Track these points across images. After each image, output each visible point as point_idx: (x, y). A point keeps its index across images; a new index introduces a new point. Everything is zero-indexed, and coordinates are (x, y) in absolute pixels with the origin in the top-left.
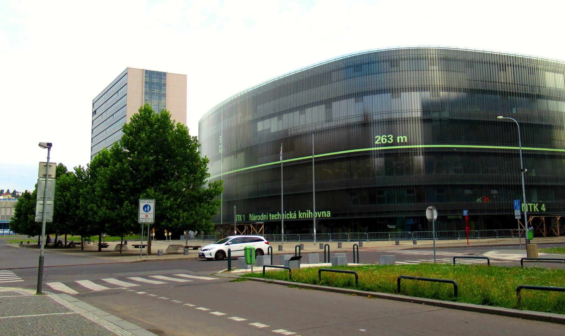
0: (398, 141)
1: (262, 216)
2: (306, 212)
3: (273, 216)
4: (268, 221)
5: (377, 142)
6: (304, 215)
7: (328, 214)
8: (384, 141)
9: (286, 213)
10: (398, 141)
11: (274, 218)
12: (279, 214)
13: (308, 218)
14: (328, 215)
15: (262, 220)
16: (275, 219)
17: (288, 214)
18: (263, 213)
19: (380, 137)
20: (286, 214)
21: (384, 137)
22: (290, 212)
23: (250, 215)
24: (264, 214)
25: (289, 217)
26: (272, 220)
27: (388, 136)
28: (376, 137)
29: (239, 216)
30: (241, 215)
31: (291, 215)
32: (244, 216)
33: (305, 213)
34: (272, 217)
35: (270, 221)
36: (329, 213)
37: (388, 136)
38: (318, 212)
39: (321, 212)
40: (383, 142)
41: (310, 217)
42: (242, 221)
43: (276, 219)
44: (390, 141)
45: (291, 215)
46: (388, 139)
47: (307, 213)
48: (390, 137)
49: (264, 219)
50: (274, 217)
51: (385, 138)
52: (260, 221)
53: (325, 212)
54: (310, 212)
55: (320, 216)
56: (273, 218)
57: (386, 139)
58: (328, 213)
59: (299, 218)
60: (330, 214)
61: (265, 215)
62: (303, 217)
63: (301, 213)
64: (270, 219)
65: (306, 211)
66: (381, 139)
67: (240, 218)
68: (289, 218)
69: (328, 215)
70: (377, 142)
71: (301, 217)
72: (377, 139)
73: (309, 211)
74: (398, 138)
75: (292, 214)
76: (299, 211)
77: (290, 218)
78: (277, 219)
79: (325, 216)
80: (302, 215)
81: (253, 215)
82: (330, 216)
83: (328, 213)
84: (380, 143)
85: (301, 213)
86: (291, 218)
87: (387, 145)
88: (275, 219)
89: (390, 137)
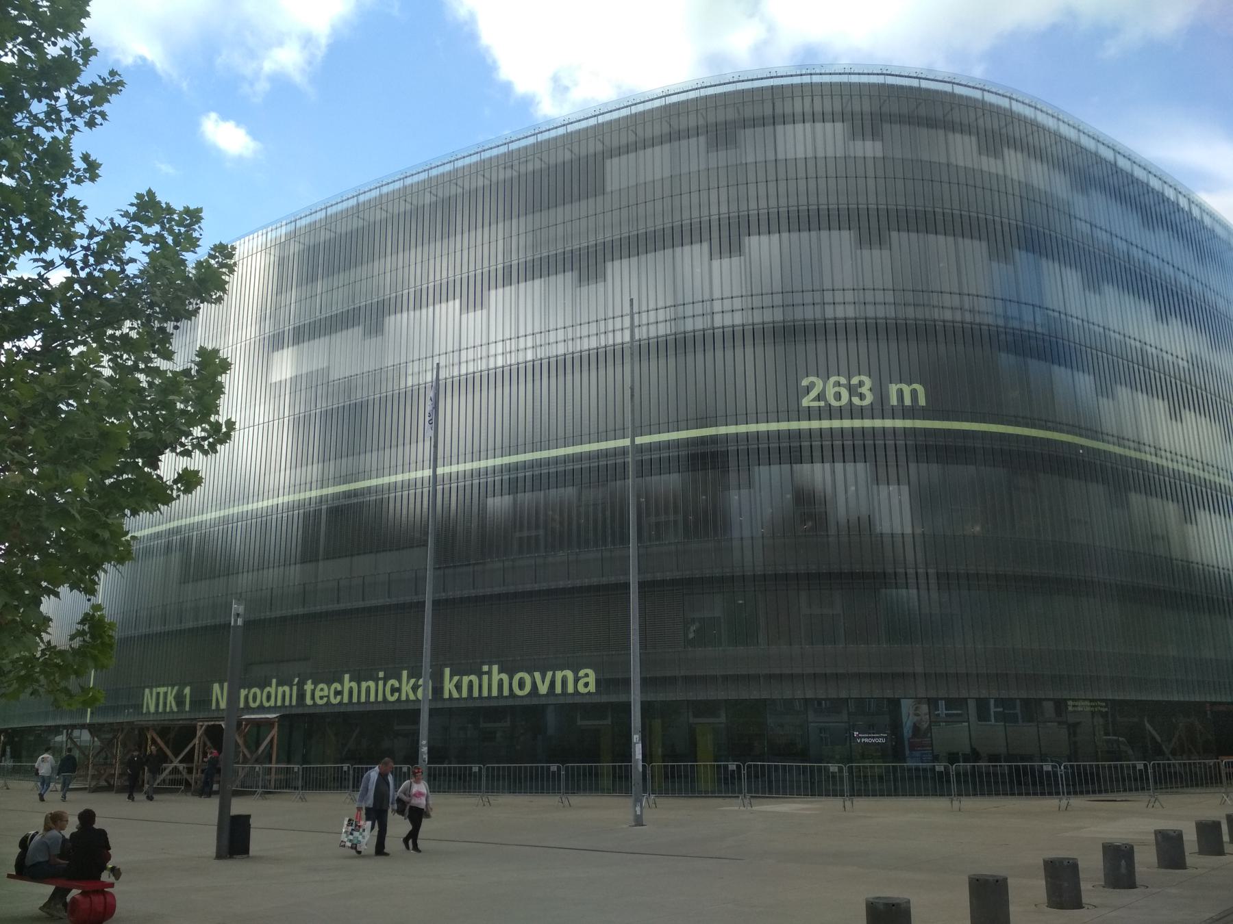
0: (894, 401)
1: (272, 690)
2: (480, 674)
3: (322, 690)
4: (300, 711)
5: (806, 402)
6: (471, 684)
7: (586, 680)
8: (838, 396)
9: (385, 680)
10: (894, 401)
11: (328, 697)
12: (351, 681)
13: (490, 697)
14: (586, 685)
15: (266, 705)
16: (328, 703)
18: (274, 681)
19: (819, 384)
20: (381, 683)
21: (838, 384)
22: (405, 673)
23: (216, 687)
24: (279, 684)
25: (396, 695)
26: (315, 704)
27: (855, 381)
28: (805, 383)
29: (166, 694)
30: (176, 688)
31: (406, 688)
32: (187, 691)
33: (474, 678)
34: (318, 694)
35: (306, 711)
36: (589, 678)
37: (855, 381)
38: (537, 675)
39: (549, 674)
40: (834, 403)
41: (495, 693)
42: (175, 709)
43: (334, 701)
44: (862, 397)
45: (406, 688)
46: (851, 390)
47: (485, 678)
48: (861, 384)
49: (279, 703)
50: (326, 693)
51: (844, 386)
52: (261, 709)
53: (569, 674)
54: (500, 672)
55: (543, 689)
56: (321, 698)
57: (845, 394)
58: (587, 675)
59: (446, 696)
60: (592, 679)
61: (287, 688)
62: (465, 694)
63: (456, 678)
64: (309, 701)
65: (481, 669)
66: (824, 390)
67: (171, 698)
68: (399, 699)
69: (586, 685)
70: (806, 402)
71: (455, 695)
72: (808, 390)
73: (495, 668)
74: (893, 388)
75: (413, 681)
76: (447, 671)
77: (404, 698)
78: (341, 703)
79: (570, 689)
80: (458, 687)
82: (592, 688)
84: (822, 404)
85: (456, 678)
86: (408, 700)
87: (852, 412)
88: (328, 703)
89: (861, 384)
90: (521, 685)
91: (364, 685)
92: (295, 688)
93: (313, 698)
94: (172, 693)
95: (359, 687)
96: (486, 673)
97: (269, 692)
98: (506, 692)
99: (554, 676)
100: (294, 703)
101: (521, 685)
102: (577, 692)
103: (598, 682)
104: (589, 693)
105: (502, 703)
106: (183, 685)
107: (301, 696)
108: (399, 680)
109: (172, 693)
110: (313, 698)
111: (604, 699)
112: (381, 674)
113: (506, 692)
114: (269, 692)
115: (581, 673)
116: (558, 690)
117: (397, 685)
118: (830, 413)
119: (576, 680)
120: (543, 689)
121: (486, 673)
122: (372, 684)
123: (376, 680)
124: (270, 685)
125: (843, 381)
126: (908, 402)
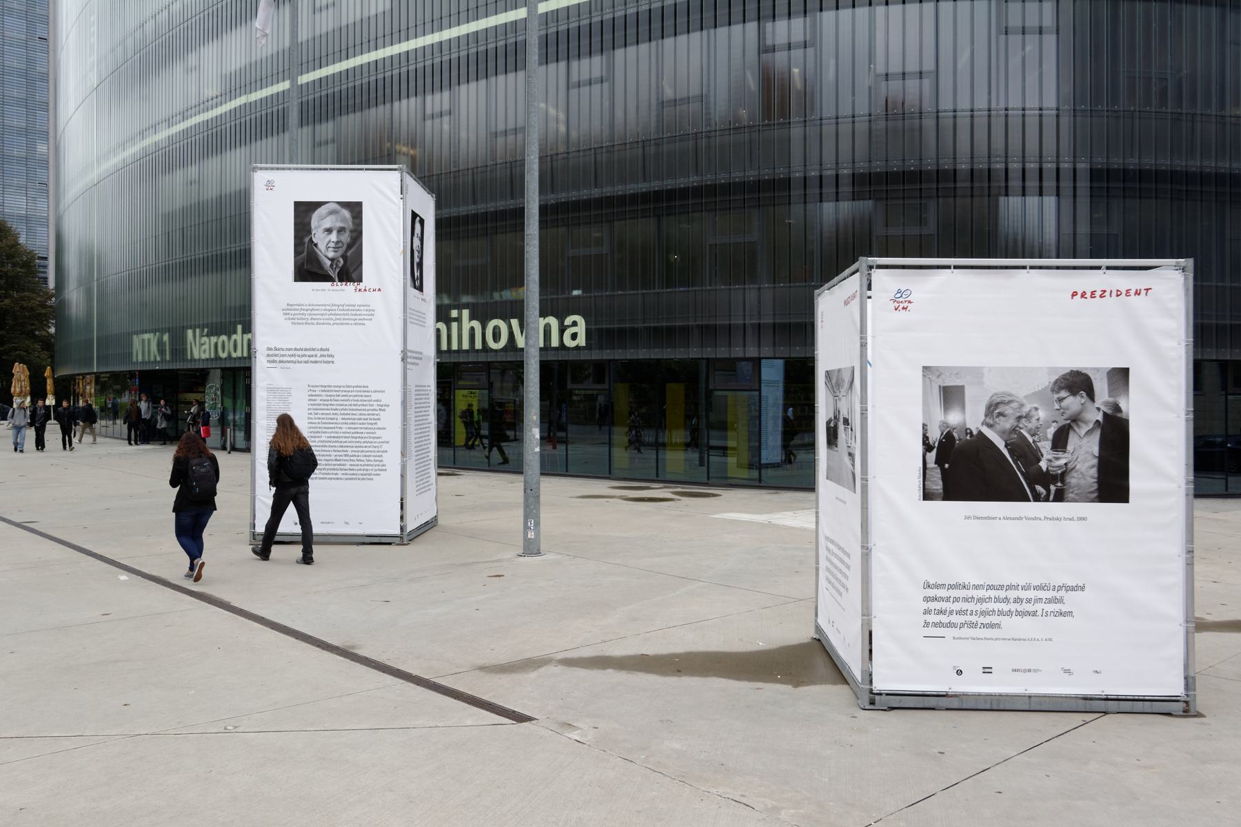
7: (573, 330)
13: (460, 351)
14: (574, 336)
18: (239, 327)
32: (166, 338)
41: (466, 346)
42: (158, 359)
47: (454, 325)
54: (472, 318)
58: (575, 324)
60: (581, 329)
67: (154, 347)
69: (574, 336)
73: (466, 313)
79: (555, 343)
82: (581, 341)
83: (575, 324)
90: (496, 336)
96: (455, 320)
98: (478, 345)
101: (496, 336)
102: (562, 345)
103: (588, 332)
104: (577, 348)
105: (472, 358)
111: (596, 355)
113: (478, 345)
115: (568, 321)
119: (562, 331)
121: (455, 320)
124: (235, 332)
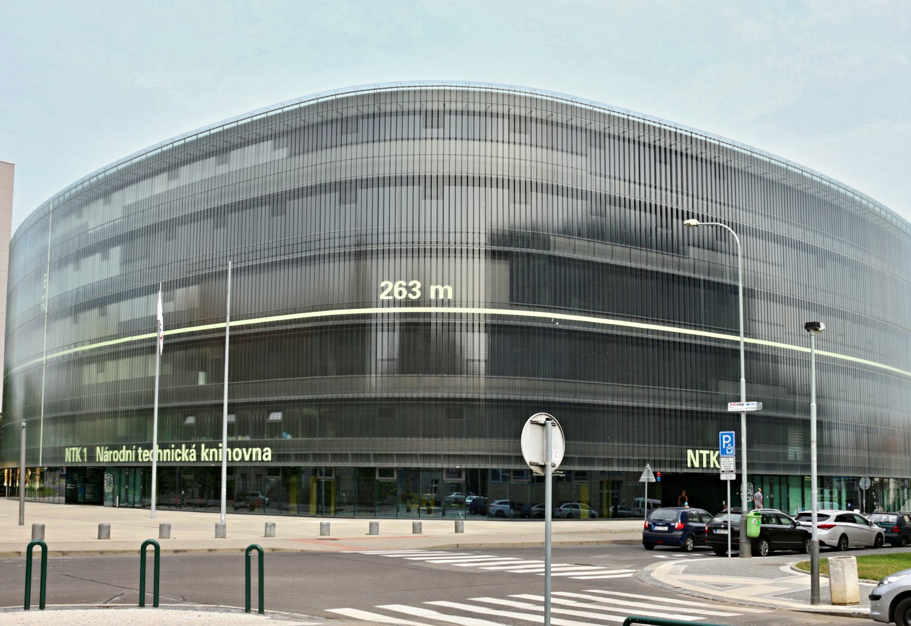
0: (433, 296)
2: (218, 448)
8: (400, 293)
9: (175, 449)
10: (433, 296)
14: (267, 456)
15: (121, 460)
17: (178, 450)
18: (124, 447)
19: (390, 284)
20: (173, 451)
21: (400, 286)
24: (127, 449)
27: (411, 284)
28: (383, 284)
32: (85, 450)
33: (215, 450)
34: (144, 455)
37: (411, 284)
38: (244, 450)
42: (80, 461)
44: (414, 294)
46: (409, 289)
48: (414, 286)
49: (127, 460)
50: (147, 455)
51: (404, 287)
53: (259, 450)
55: (247, 458)
56: (146, 457)
58: (267, 451)
59: (202, 460)
60: (269, 453)
62: (211, 459)
64: (140, 460)
66: (393, 289)
67: (78, 456)
69: (267, 456)
72: (383, 289)
74: (433, 289)
76: (203, 445)
80: (208, 455)
81: (104, 450)
82: (269, 458)
83: (267, 451)
84: (391, 298)
87: (408, 303)
89: (414, 286)
90: (237, 455)
91: (165, 451)
92: (134, 451)
93: (142, 458)
94: (78, 450)
95: (163, 452)
97: (122, 453)
99: (252, 451)
100: (134, 460)
101: (237, 455)
102: (262, 460)
104: (268, 461)
106: (83, 447)
107: (137, 456)
108: (181, 449)
109: (78, 450)
110: (142, 458)
112: (173, 446)
114: (122, 453)
115: (265, 450)
116: (254, 459)
117: (180, 452)
118: (395, 303)
120: (247, 458)
122: (168, 451)
123: (171, 449)
124: (122, 449)
125: (404, 283)
126: (441, 296)
